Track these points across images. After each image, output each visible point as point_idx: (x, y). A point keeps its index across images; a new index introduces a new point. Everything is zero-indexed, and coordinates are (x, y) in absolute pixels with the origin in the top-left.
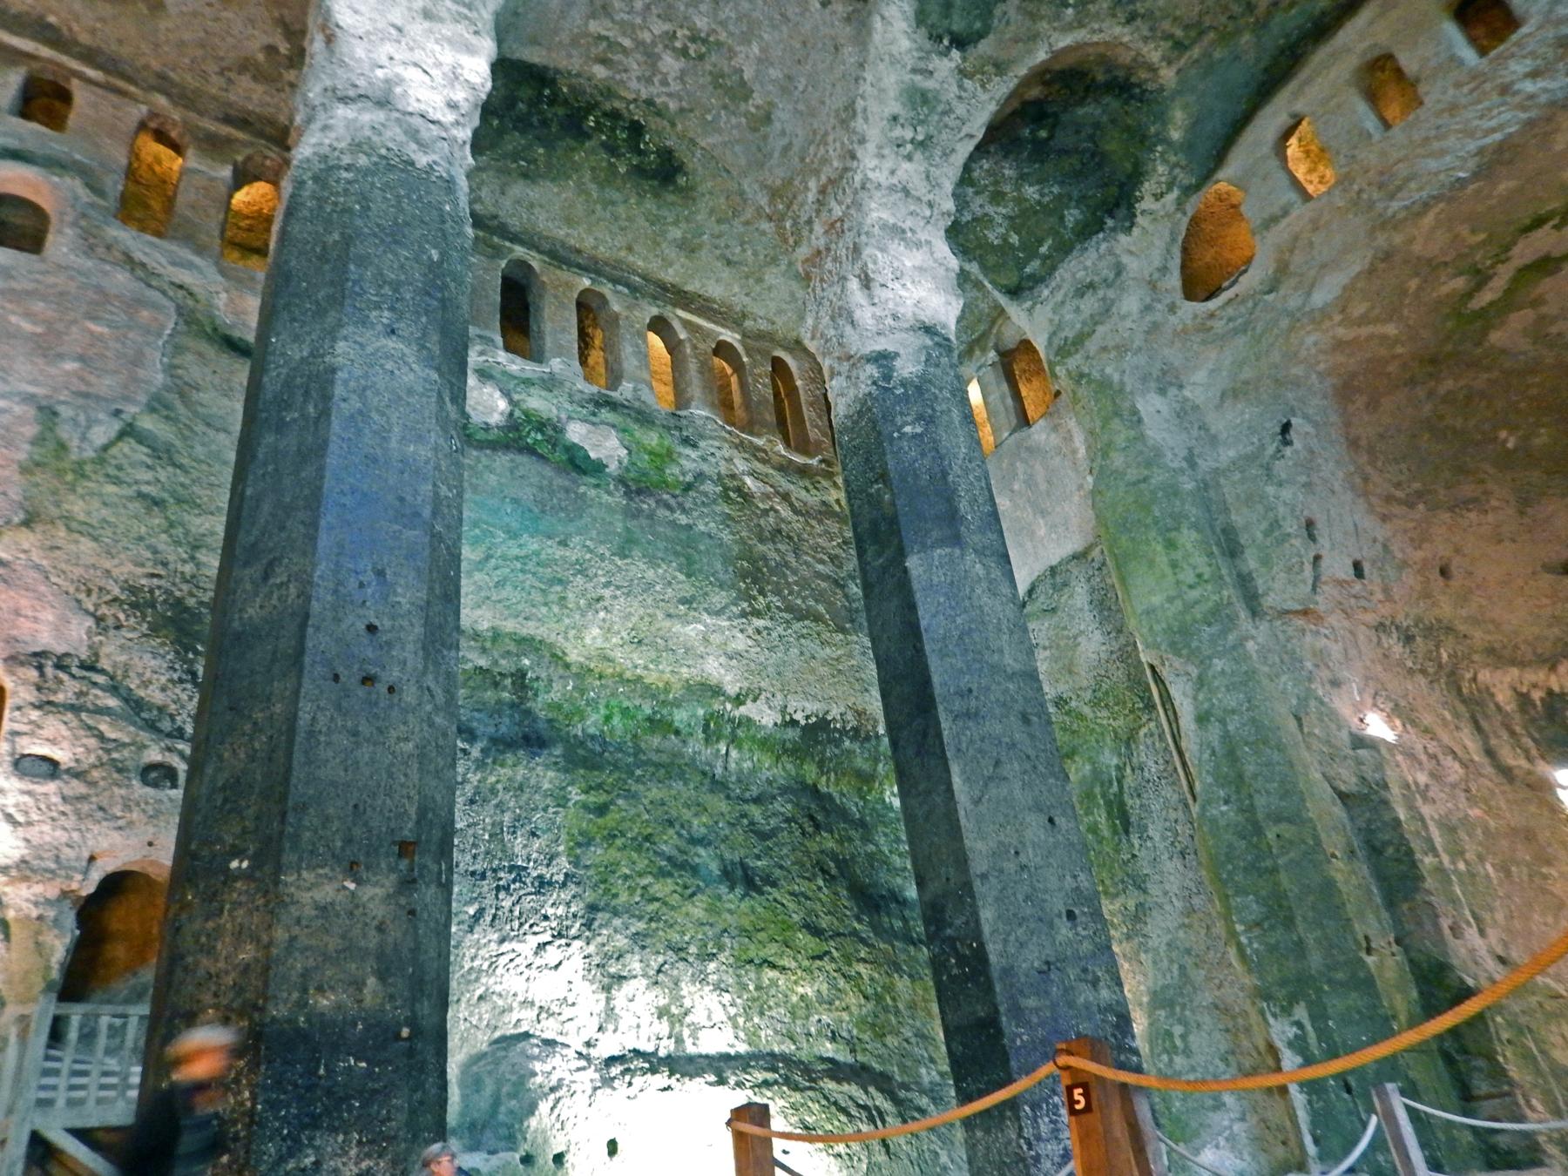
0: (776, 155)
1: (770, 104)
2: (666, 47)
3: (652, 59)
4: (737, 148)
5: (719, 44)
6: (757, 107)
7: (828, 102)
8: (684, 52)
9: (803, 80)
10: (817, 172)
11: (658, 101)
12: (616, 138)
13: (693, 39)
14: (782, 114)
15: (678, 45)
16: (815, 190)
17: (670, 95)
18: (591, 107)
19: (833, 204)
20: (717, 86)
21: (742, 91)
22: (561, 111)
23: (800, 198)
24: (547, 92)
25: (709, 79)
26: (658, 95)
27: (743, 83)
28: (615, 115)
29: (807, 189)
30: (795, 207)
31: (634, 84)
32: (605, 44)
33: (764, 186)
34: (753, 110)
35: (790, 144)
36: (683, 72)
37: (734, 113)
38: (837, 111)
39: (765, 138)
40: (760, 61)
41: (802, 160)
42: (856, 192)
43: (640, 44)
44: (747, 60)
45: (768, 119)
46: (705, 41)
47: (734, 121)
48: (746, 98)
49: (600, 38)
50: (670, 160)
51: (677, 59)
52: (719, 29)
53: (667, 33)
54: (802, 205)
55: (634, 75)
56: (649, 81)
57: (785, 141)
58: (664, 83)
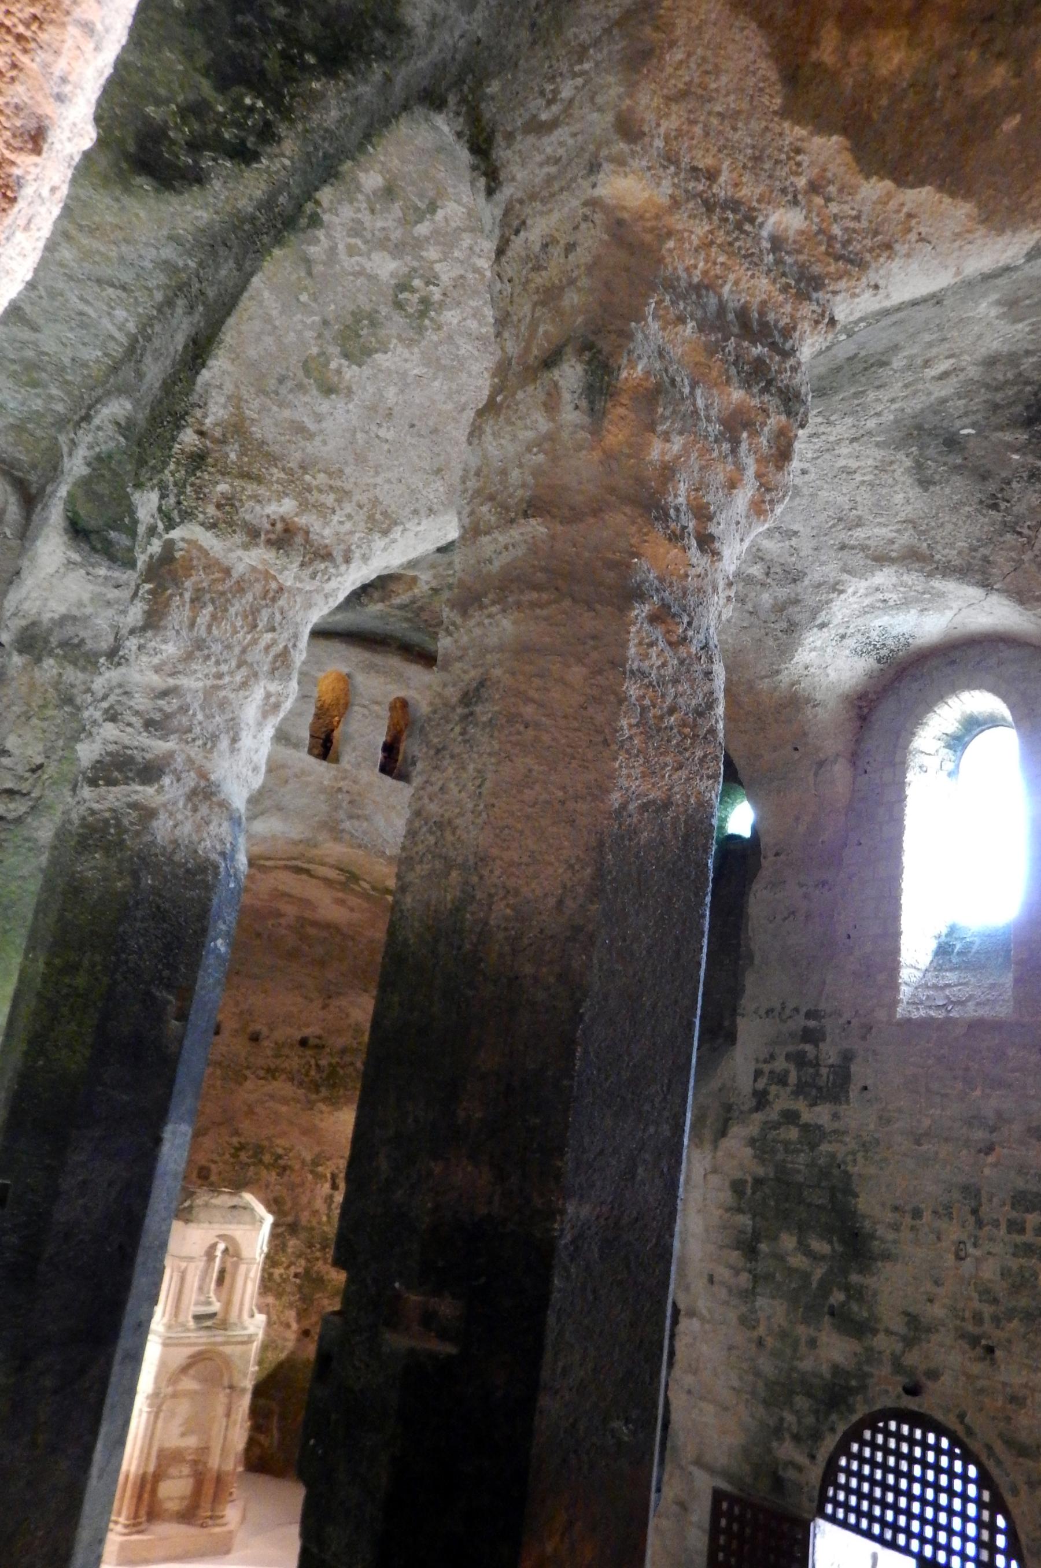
0: (287, 413)
1: (350, 392)
2: (414, 270)
3: (398, 250)
4: (269, 340)
5: (421, 330)
6: (339, 372)
7: (379, 480)
8: (403, 286)
9: (390, 435)
10: (304, 506)
11: (321, 234)
12: (220, 124)
13: (425, 301)
14: (338, 417)
15: (417, 283)
16: (282, 510)
17: (333, 250)
18: (285, 113)
19: (295, 567)
20: (357, 316)
21: (357, 351)
22: (273, 65)
23: (262, 491)
24: (311, 59)
25: (368, 308)
26: (329, 236)
27: (368, 352)
28: (267, 134)
29: (280, 496)
30: (251, 488)
31: (347, 212)
32: (422, 206)
33: (236, 401)
34: (333, 365)
35: (310, 436)
36: (372, 278)
37: (320, 336)
38: (375, 502)
39: (300, 387)
40: (404, 375)
41: (304, 468)
42: (317, 591)
43: (419, 244)
44: (397, 358)
45: (328, 390)
46: (423, 314)
47: (309, 334)
48: (346, 355)
49: (432, 208)
50: (183, 177)
51: (392, 275)
52: (442, 334)
53: (436, 277)
54: (257, 499)
55: (366, 218)
56: (356, 229)
57: (312, 427)
58: (351, 251)
